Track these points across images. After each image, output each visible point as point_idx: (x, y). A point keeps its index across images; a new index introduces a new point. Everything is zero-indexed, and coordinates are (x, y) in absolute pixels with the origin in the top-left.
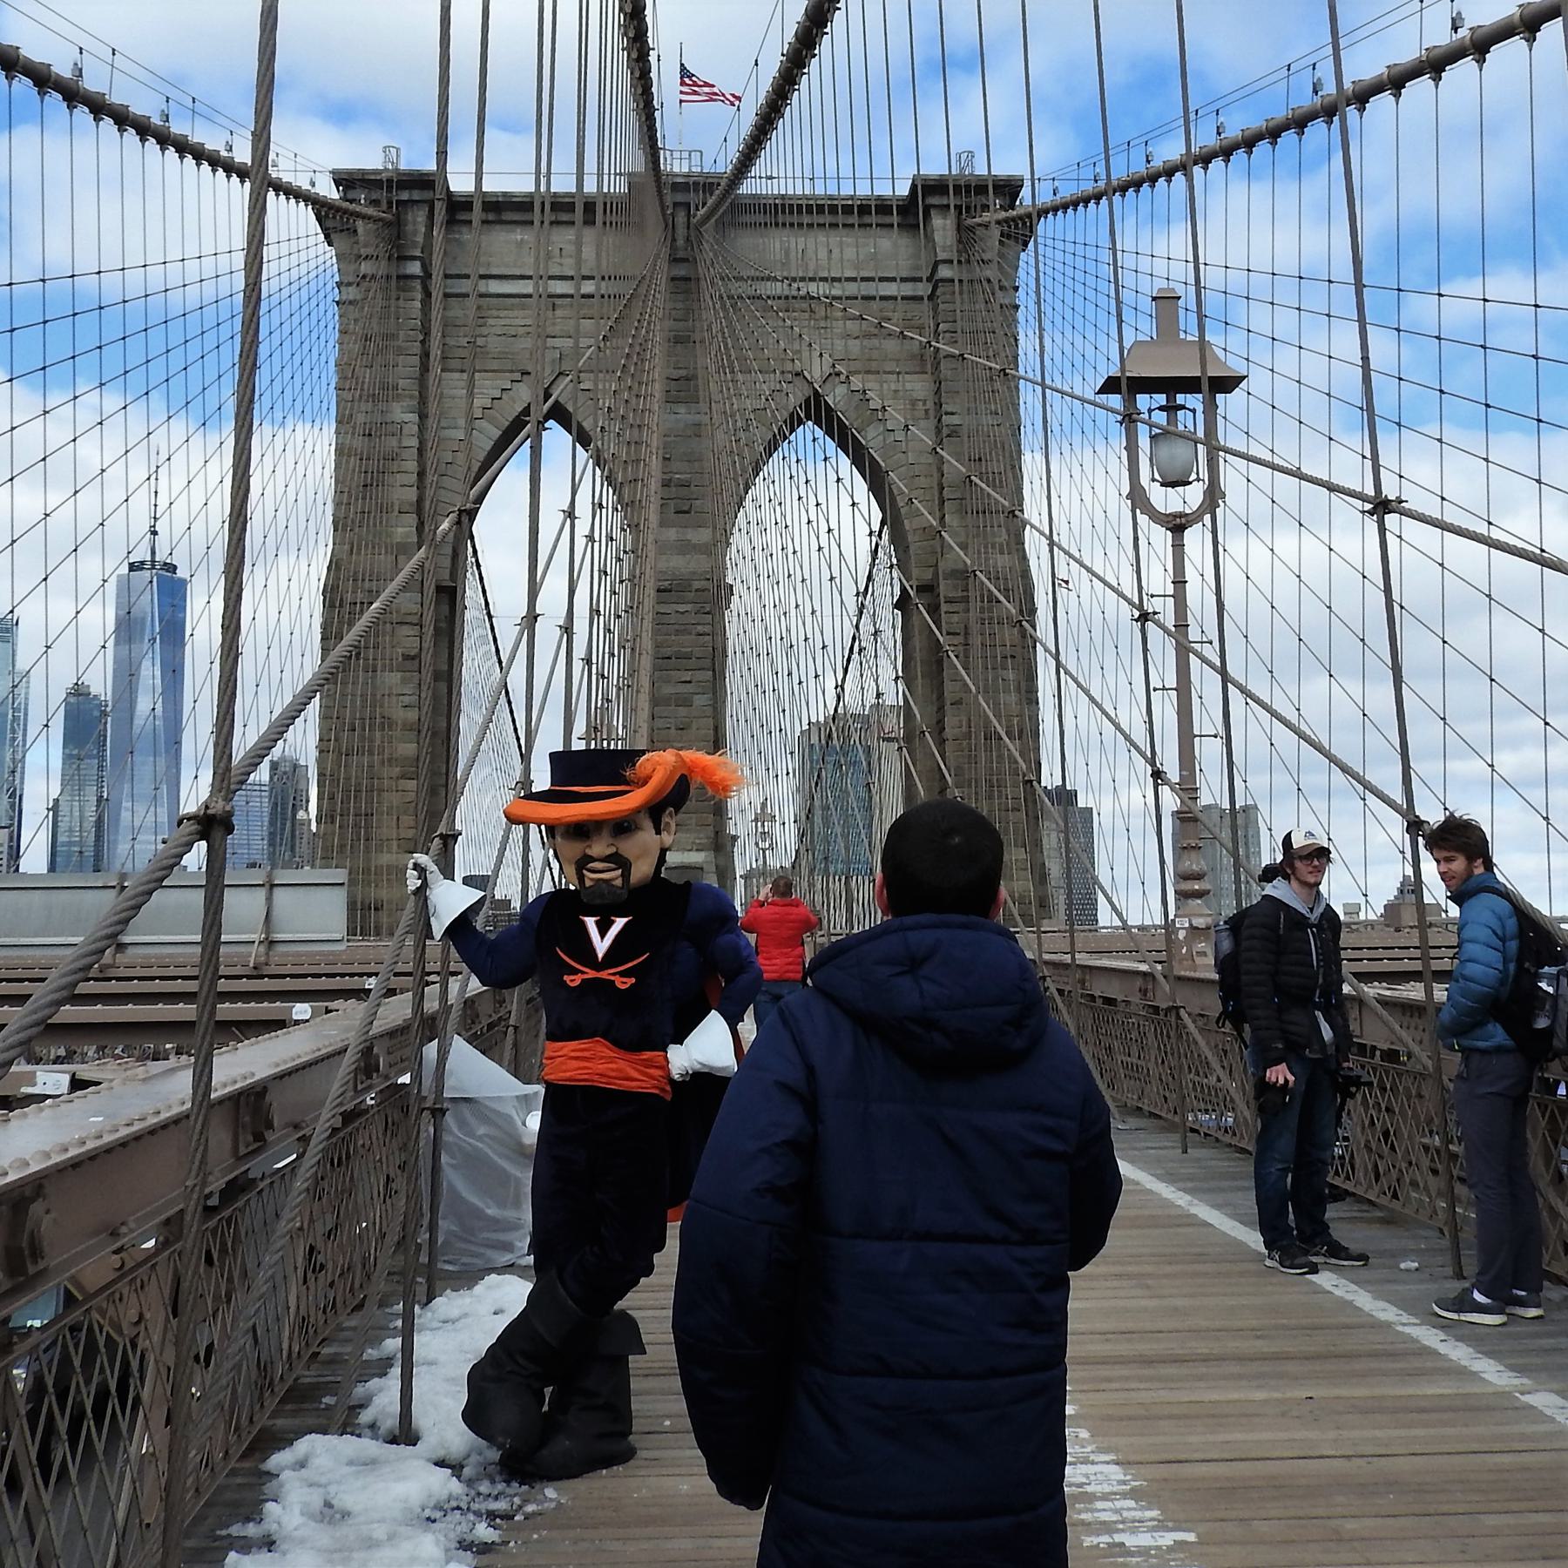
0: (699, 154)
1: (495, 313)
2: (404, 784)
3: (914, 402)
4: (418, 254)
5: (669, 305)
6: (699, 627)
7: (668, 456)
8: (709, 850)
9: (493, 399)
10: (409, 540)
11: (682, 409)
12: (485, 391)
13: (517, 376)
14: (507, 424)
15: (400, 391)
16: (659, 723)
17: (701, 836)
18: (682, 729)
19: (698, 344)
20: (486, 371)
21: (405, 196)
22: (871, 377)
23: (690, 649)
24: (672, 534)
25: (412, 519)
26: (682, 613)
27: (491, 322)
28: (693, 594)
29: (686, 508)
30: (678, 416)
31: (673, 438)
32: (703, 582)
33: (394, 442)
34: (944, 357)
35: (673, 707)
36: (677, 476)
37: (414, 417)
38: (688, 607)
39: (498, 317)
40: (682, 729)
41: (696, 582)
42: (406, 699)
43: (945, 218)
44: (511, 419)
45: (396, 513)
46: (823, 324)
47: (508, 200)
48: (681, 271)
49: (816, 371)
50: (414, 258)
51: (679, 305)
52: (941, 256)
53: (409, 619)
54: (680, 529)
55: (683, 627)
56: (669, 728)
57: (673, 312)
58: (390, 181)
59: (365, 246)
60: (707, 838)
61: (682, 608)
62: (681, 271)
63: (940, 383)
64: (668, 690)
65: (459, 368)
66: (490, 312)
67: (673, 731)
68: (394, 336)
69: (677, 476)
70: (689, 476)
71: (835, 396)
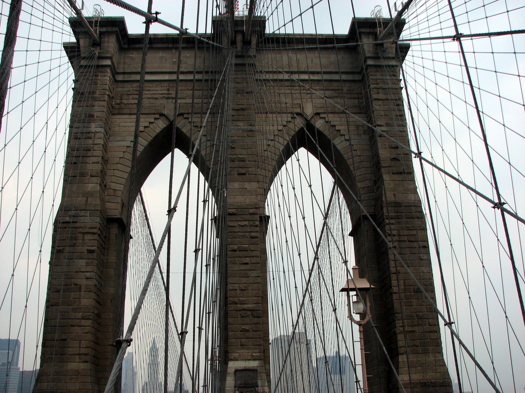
2: (84, 322)
3: (357, 127)
4: (109, 55)
8: (259, 360)
11: (240, 124)
13: (157, 116)
14: (152, 138)
15: (95, 118)
17: (256, 351)
21: (104, 29)
22: (336, 115)
25: (98, 180)
26: (242, 226)
29: (243, 172)
30: (239, 127)
33: (90, 141)
36: (239, 156)
37: (102, 130)
38: (246, 223)
39: (149, 90)
40: (243, 290)
42: (88, 275)
43: (368, 38)
44: (153, 136)
45: (89, 176)
47: (156, 37)
49: (309, 111)
50: (106, 58)
52: (368, 55)
54: (241, 183)
56: (236, 290)
58: (96, 22)
59: (84, 53)
65: (129, 113)
67: (239, 291)
68: (94, 93)
69: (239, 156)
71: (319, 124)
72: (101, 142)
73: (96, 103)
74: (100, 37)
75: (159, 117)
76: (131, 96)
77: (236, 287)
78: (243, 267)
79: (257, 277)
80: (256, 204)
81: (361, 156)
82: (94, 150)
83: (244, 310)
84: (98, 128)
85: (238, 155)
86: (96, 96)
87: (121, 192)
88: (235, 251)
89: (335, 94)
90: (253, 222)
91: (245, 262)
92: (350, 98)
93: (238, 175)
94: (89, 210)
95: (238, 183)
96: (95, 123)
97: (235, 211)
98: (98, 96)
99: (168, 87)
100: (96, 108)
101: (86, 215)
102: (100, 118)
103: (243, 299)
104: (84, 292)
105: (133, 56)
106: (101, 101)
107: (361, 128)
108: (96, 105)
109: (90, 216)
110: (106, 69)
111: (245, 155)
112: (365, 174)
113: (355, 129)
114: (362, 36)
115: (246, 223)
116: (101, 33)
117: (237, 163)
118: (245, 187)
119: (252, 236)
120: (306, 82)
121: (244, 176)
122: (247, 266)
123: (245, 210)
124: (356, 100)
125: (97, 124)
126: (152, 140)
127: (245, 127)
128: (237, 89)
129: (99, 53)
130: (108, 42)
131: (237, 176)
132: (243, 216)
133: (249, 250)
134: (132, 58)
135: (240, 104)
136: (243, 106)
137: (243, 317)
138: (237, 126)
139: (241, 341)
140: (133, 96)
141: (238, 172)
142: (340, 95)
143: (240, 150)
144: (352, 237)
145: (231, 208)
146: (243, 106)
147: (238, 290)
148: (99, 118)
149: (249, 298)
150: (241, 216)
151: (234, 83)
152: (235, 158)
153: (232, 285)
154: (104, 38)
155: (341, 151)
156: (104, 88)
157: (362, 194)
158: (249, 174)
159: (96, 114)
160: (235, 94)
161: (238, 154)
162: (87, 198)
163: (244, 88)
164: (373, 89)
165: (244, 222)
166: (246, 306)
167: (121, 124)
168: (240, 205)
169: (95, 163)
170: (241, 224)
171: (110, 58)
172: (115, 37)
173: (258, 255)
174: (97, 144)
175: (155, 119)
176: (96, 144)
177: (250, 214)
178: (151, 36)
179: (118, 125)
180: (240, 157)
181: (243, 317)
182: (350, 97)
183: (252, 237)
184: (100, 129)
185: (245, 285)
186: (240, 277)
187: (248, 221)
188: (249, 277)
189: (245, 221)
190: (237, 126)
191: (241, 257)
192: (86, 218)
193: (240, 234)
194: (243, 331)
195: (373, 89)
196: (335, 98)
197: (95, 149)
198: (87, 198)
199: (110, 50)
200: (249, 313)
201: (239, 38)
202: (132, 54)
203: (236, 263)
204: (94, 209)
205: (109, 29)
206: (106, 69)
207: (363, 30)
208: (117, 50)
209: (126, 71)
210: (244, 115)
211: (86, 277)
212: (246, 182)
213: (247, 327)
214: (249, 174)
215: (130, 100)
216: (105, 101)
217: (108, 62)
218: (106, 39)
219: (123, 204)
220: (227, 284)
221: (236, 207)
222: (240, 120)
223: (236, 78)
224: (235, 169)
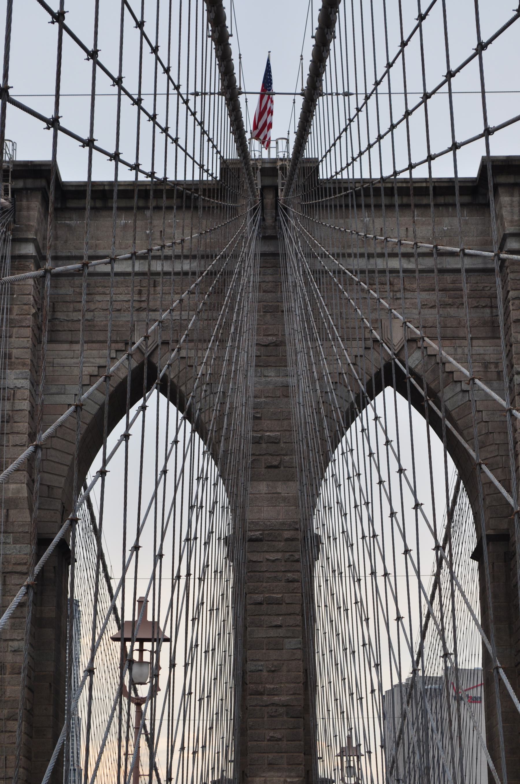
0: (285, 141)
1: (101, 290)
4: (31, 236)
5: (258, 279)
6: (289, 575)
7: (258, 416)
9: (99, 367)
10: (21, 495)
11: (271, 372)
12: (92, 360)
16: (250, 666)
17: (292, 774)
18: (273, 671)
19: (285, 313)
20: (93, 342)
21: (20, 184)
22: (447, 342)
23: (280, 596)
24: (263, 487)
26: (273, 561)
27: (98, 298)
28: (282, 543)
29: (275, 463)
30: (269, 379)
31: (263, 399)
32: (292, 533)
34: (514, 322)
35: (264, 651)
36: (268, 434)
38: (279, 556)
40: (273, 671)
41: (286, 532)
43: (512, 195)
46: (398, 295)
48: (269, 248)
50: (27, 240)
51: (270, 278)
53: (19, 568)
54: (270, 483)
55: (273, 575)
56: (261, 670)
57: (263, 285)
60: (298, 777)
61: (272, 556)
62: (269, 248)
63: (511, 346)
64: (261, 633)
65: (70, 339)
66: (97, 289)
67: (265, 673)
69: (268, 434)
70: (279, 433)
72: (25, 405)
73: (15, 330)
74: (13, 202)
75: (124, 349)
76: (72, 306)
77: (262, 665)
78: (273, 633)
79: (296, 649)
80: (296, 523)
81: (490, 423)
82: (15, 422)
83: (273, 704)
84: (20, 381)
85: (267, 431)
86: (12, 317)
87: (60, 491)
88: (261, 604)
89: (447, 299)
90: (290, 553)
91: (275, 623)
92: (477, 307)
93: (266, 468)
94: (12, 533)
95: (265, 483)
96: (12, 369)
97: (261, 534)
98: (17, 317)
99: (139, 288)
100: (13, 339)
101: (8, 541)
102: (23, 360)
103: (272, 686)
104: (9, 674)
105: (73, 223)
106: (22, 326)
107: (492, 368)
108: (14, 336)
109: (14, 543)
110: (28, 264)
111: (278, 431)
112: (494, 457)
113: (481, 370)
114: (500, 190)
115: (279, 556)
116: (14, 191)
117: (264, 446)
118: (279, 491)
119: (288, 579)
120: (394, 275)
121: (276, 471)
122: (280, 630)
123: (277, 532)
124: (488, 310)
125: (18, 371)
126: (113, 391)
127: (277, 379)
128: (265, 304)
129: (13, 230)
130: (29, 209)
131: (264, 469)
132: (274, 543)
133: (284, 604)
134: (69, 227)
135: (270, 333)
136: (274, 339)
137: (272, 716)
138: (265, 376)
139: (268, 757)
140: (75, 304)
141: (265, 464)
142: (456, 300)
143: (268, 422)
144: (478, 563)
145: (254, 528)
146: (274, 339)
147: (265, 670)
148: (20, 360)
149: (282, 685)
150: (270, 543)
151: (259, 292)
152: (260, 437)
153: (254, 663)
154: (21, 201)
155: (453, 412)
156: (25, 302)
157: (487, 495)
158: (285, 467)
159: (15, 352)
160: (262, 314)
161: (266, 429)
162: (8, 510)
163: (278, 301)
164: (513, 299)
165: (274, 554)
166: (276, 698)
167: (56, 361)
168: (269, 523)
169: (17, 445)
170: (271, 558)
171: (34, 241)
172: (40, 197)
173: (297, 612)
174: (20, 410)
175: (117, 351)
176: (17, 410)
177: (287, 540)
178: (104, 185)
179: (50, 363)
180: (269, 436)
181: (272, 716)
182: (476, 305)
183: (289, 581)
184: (22, 381)
185: (275, 663)
186: (267, 649)
187: (282, 551)
188: (282, 649)
189: (278, 551)
190: (265, 376)
191: (269, 615)
192: (8, 546)
193: (267, 575)
194: (273, 741)
195: (513, 299)
196: (449, 307)
197: (16, 420)
198: (8, 510)
199: (32, 224)
200: (281, 710)
201: (269, 199)
202: (71, 219)
203: (261, 626)
204: (20, 530)
205: (30, 183)
206: (28, 264)
207: (502, 179)
208: (42, 216)
209: (60, 254)
210: (277, 356)
211: (13, 649)
212: (280, 481)
213: (278, 735)
214: (285, 467)
215: (70, 314)
216: (29, 327)
217: (30, 249)
218: (24, 203)
219: (64, 507)
220: (246, 661)
221: (261, 528)
222: (270, 364)
223: (264, 281)
224: (261, 457)
